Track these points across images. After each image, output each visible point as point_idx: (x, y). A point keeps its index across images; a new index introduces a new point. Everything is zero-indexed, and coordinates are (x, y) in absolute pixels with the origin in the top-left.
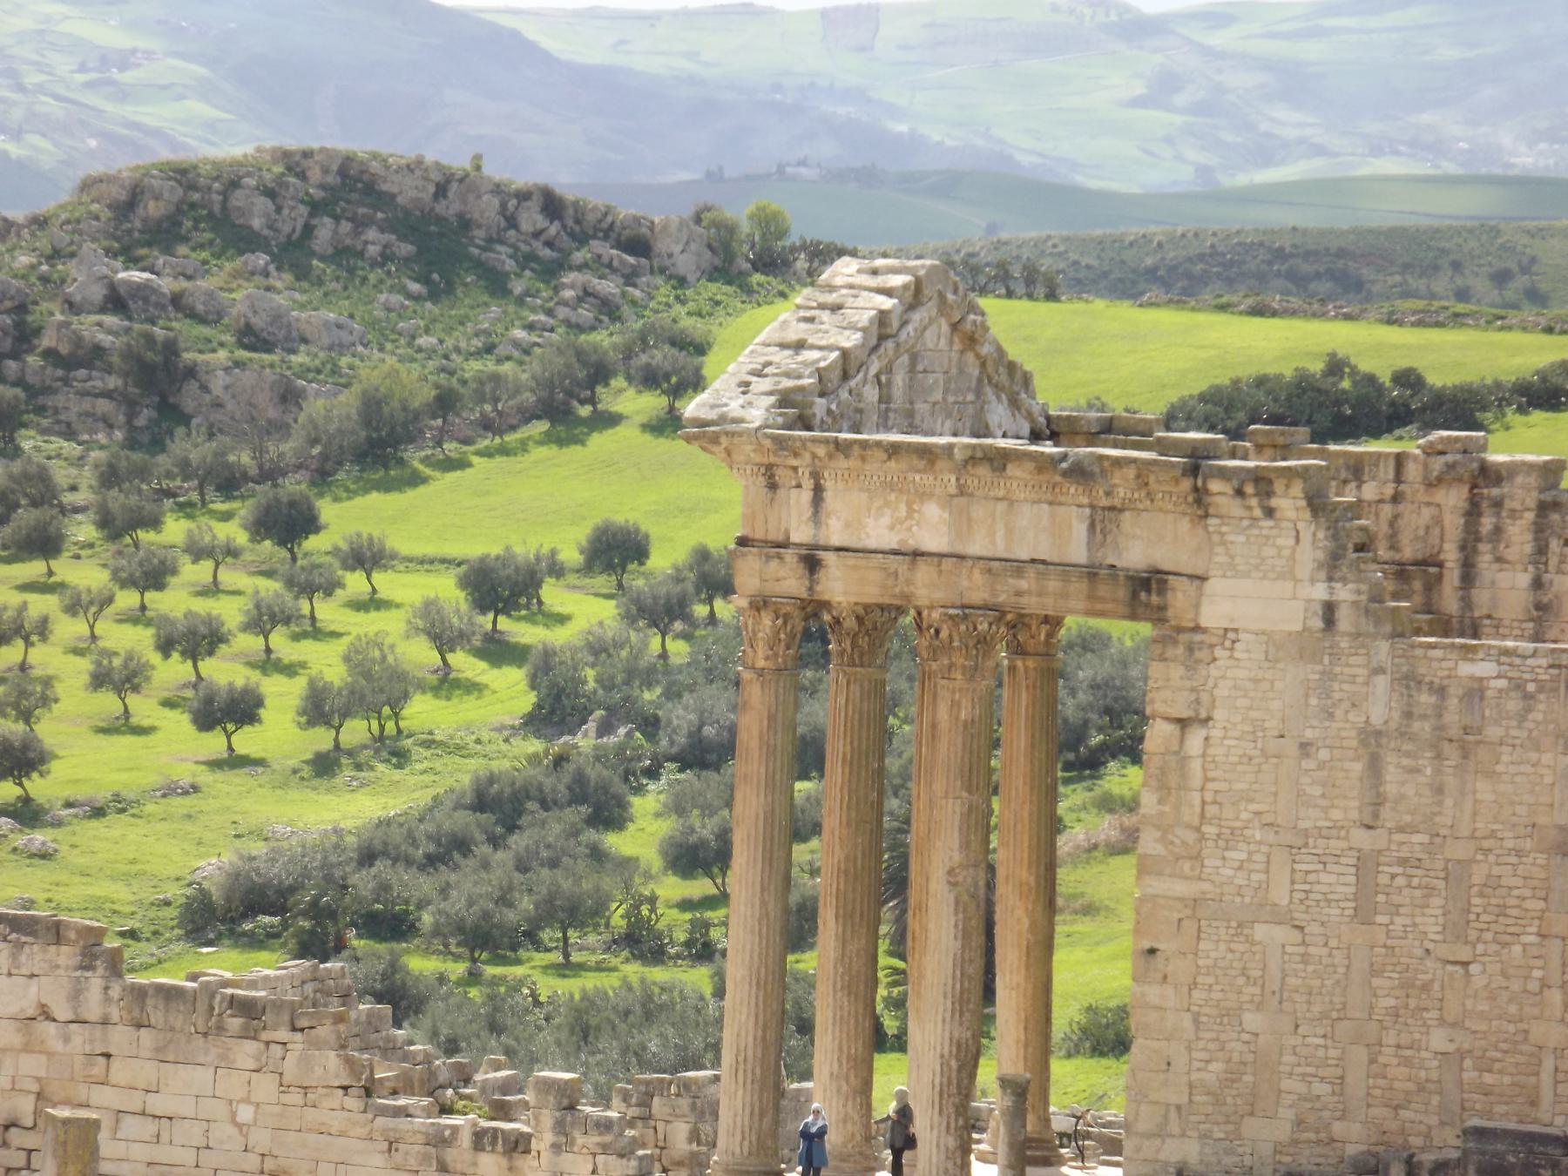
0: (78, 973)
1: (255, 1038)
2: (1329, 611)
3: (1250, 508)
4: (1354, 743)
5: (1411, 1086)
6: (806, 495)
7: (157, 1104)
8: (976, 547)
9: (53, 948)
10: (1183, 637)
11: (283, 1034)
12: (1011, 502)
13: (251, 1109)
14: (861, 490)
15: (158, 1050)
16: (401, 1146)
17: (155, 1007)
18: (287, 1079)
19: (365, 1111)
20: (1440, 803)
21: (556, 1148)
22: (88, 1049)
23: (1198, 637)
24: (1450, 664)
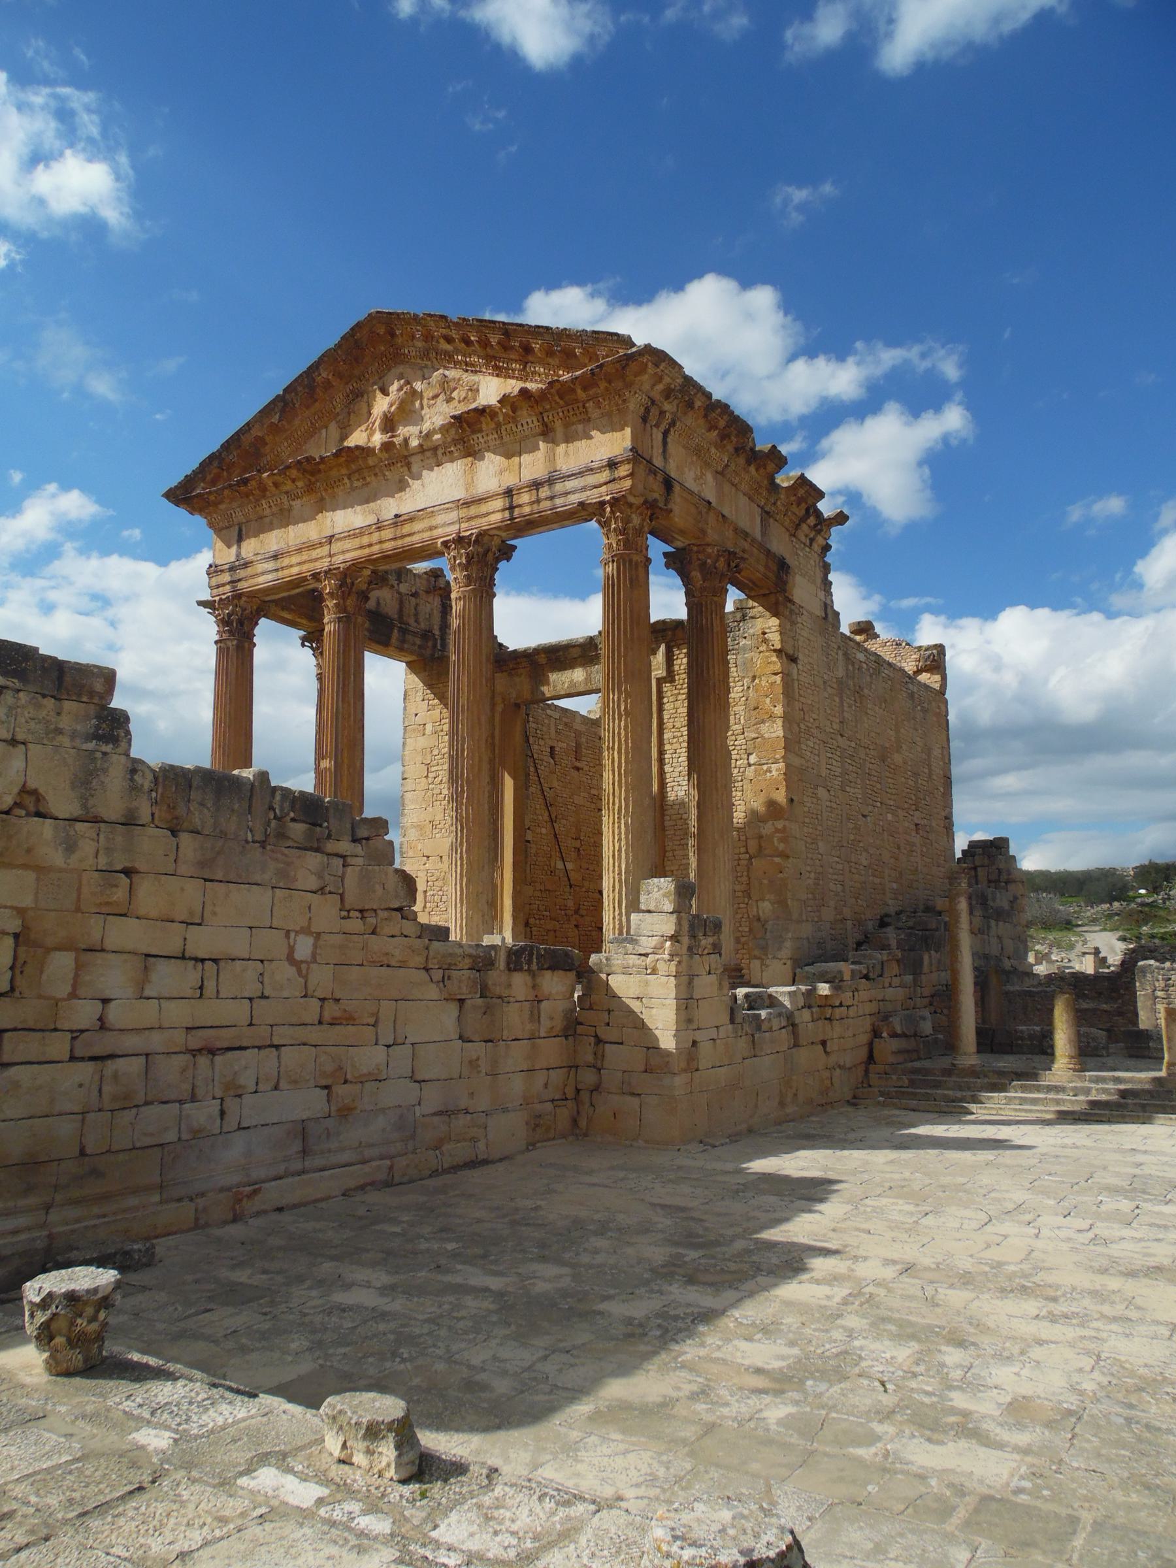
0: (91, 745)
1: (317, 850)
2: (826, 605)
3: (806, 536)
4: (835, 686)
5: (858, 885)
6: (660, 436)
7: (202, 942)
8: (726, 512)
9: (50, 703)
10: (789, 605)
11: (344, 846)
12: (737, 489)
13: (310, 941)
14: (684, 447)
15: (202, 864)
16: (454, 974)
17: (202, 804)
18: (351, 899)
19: (419, 937)
20: (856, 726)
21: (690, 949)
22: (103, 862)
23: (793, 607)
24: (854, 651)
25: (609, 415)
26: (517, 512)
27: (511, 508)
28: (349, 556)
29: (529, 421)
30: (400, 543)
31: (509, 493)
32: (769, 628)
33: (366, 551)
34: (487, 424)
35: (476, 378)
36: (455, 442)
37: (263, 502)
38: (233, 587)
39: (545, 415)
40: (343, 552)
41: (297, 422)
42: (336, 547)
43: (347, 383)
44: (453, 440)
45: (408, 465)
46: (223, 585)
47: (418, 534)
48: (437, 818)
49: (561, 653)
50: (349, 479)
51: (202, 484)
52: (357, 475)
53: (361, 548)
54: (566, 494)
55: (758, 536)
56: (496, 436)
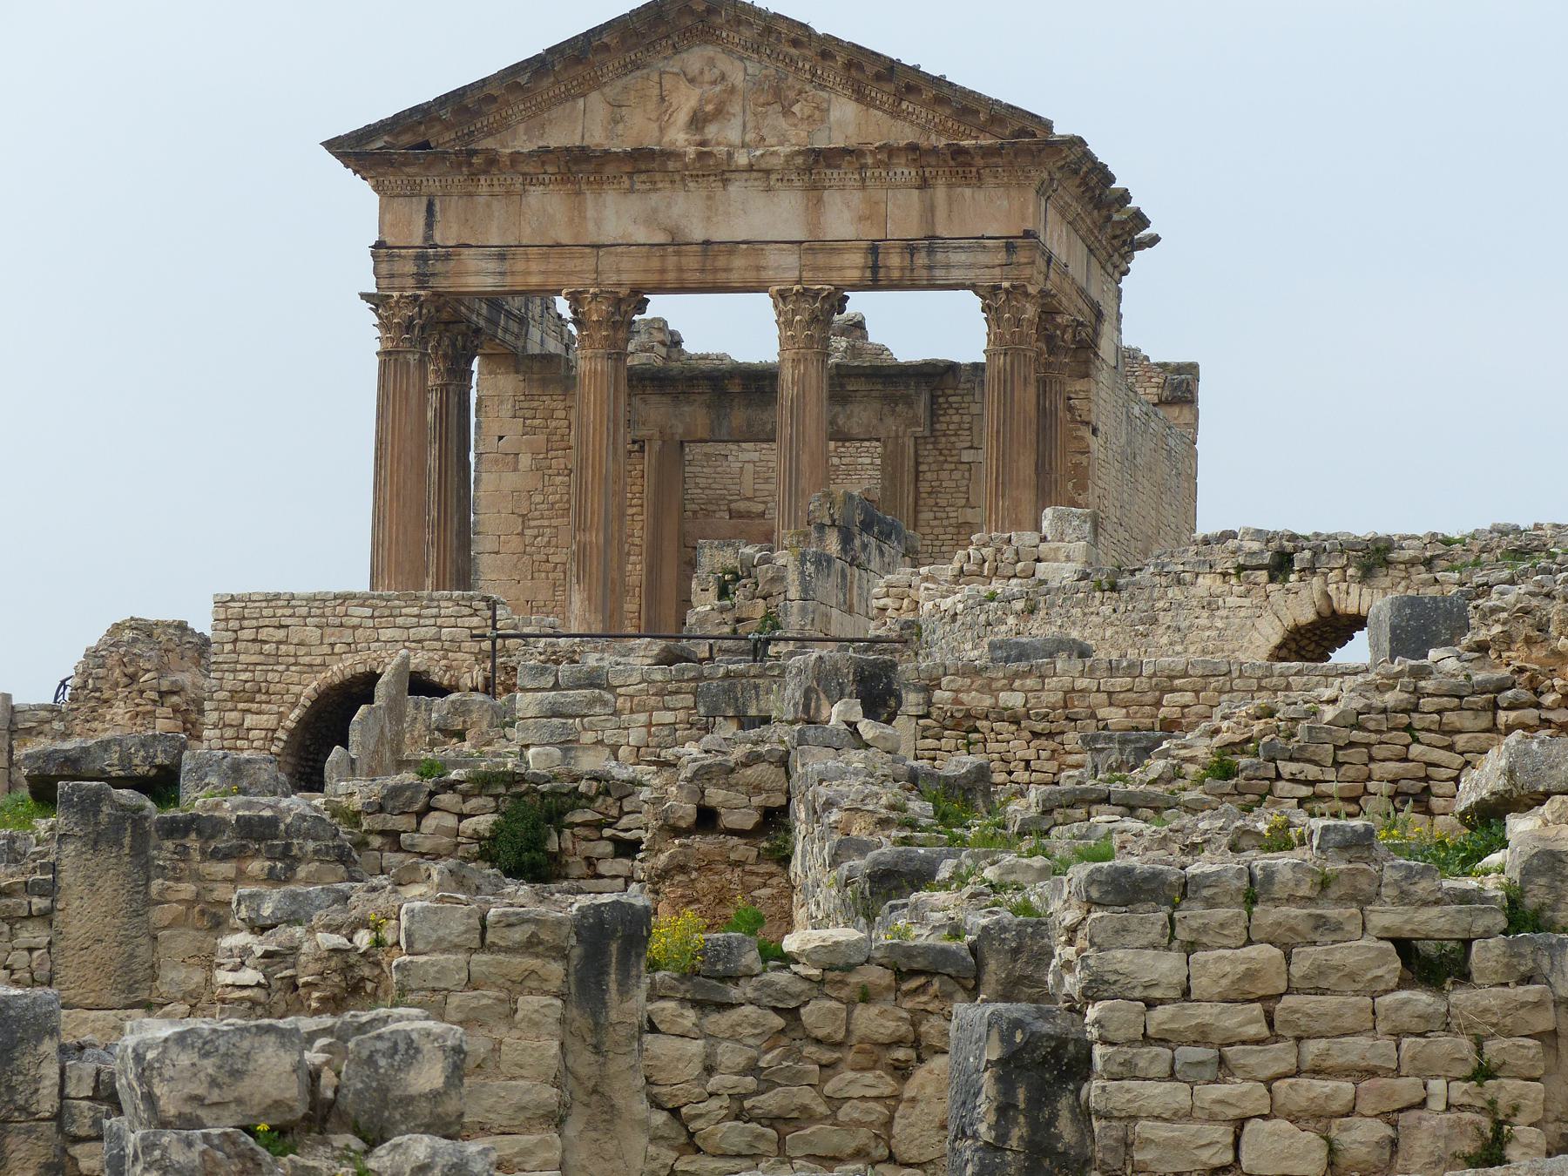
25: (1007, 186)
26: (882, 273)
27: (875, 268)
28: (626, 278)
29: (906, 172)
30: (709, 277)
31: (874, 250)
32: (1076, 392)
34: (849, 163)
35: (824, 95)
36: (801, 171)
37: (482, 178)
38: (419, 281)
39: (927, 170)
40: (619, 271)
41: (547, 82)
42: (607, 261)
43: (628, 51)
44: (797, 168)
45: (726, 182)
46: (402, 275)
48: (540, 597)
49: (767, 382)
50: (631, 178)
51: (386, 138)
52: (643, 177)
53: (645, 271)
54: (948, 266)
55: (1085, 285)
56: (857, 176)
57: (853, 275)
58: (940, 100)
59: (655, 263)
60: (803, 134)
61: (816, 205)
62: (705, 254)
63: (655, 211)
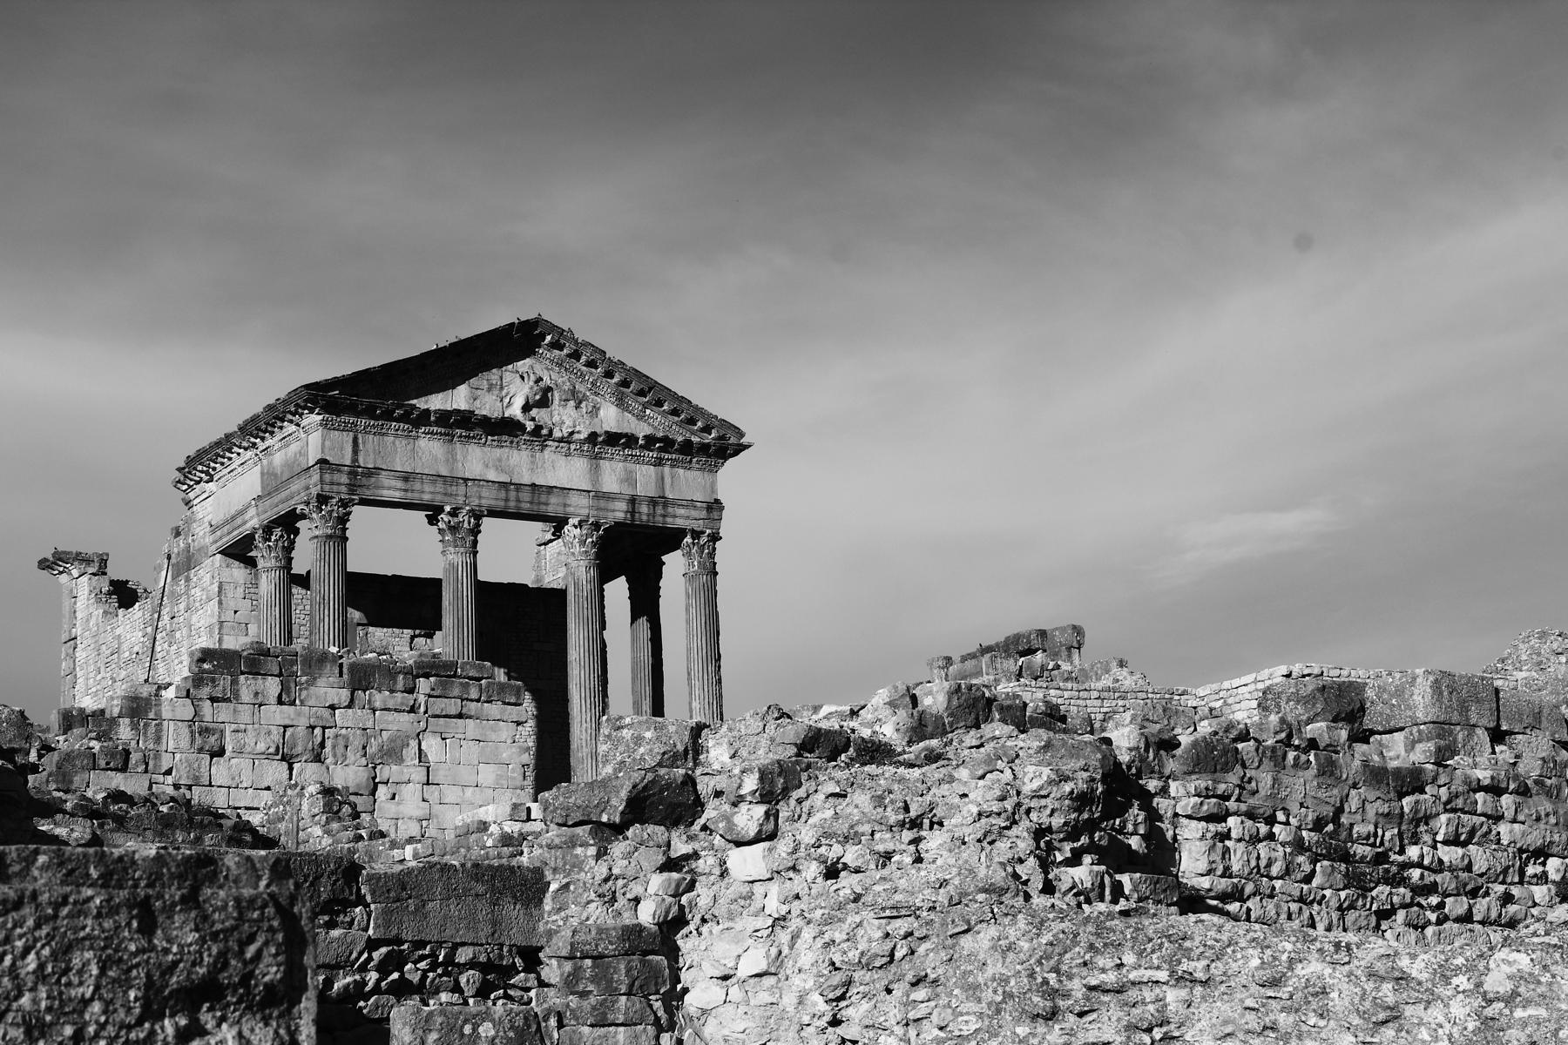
27: (633, 513)
28: (484, 502)
30: (535, 508)
31: (633, 501)
33: (502, 504)
38: (350, 490)
42: (473, 489)
45: (543, 447)
46: (339, 484)
47: (553, 506)
54: (675, 516)
57: (620, 516)
58: (675, 412)
59: (503, 494)
60: (588, 422)
61: (595, 471)
62: (533, 492)
63: (500, 460)
